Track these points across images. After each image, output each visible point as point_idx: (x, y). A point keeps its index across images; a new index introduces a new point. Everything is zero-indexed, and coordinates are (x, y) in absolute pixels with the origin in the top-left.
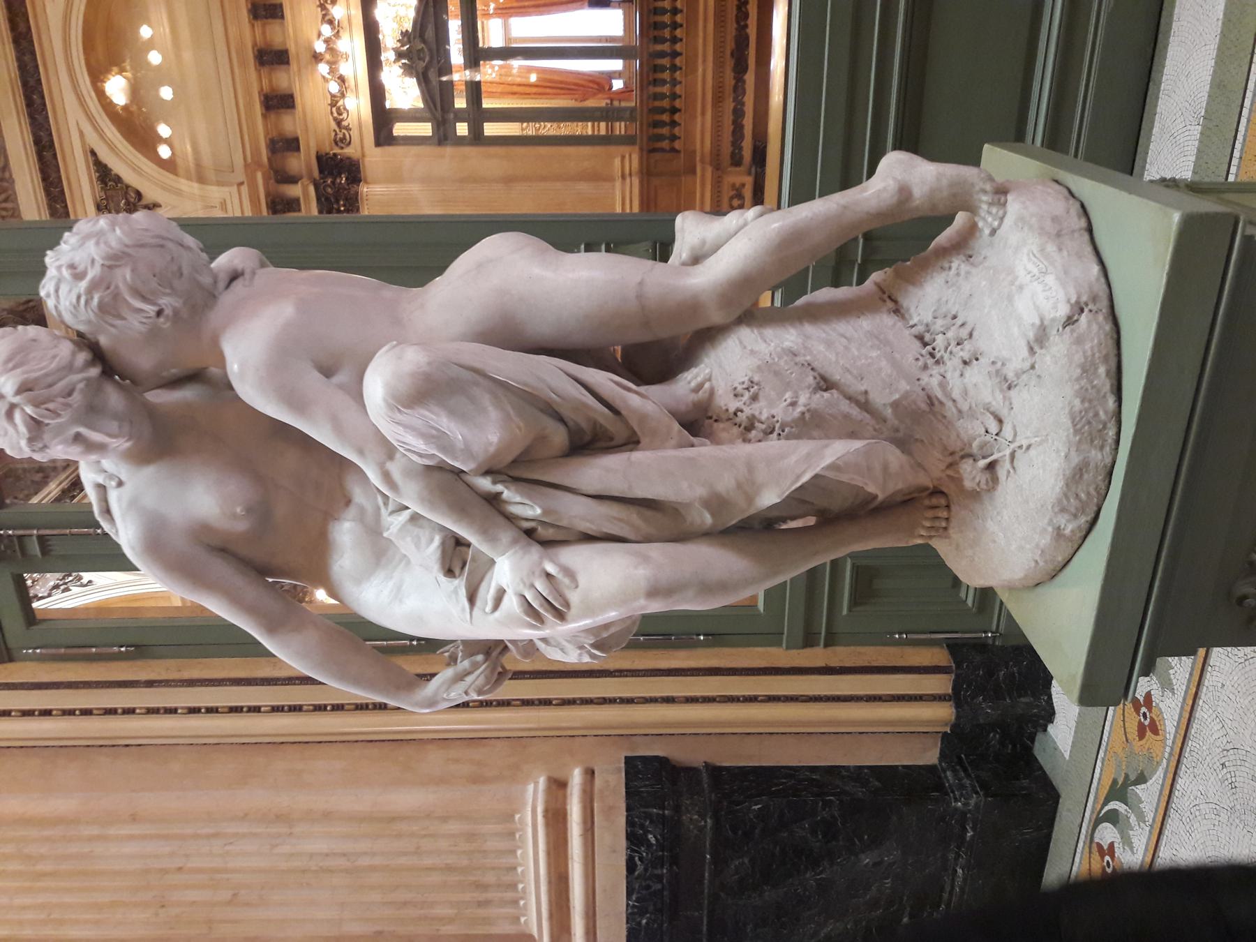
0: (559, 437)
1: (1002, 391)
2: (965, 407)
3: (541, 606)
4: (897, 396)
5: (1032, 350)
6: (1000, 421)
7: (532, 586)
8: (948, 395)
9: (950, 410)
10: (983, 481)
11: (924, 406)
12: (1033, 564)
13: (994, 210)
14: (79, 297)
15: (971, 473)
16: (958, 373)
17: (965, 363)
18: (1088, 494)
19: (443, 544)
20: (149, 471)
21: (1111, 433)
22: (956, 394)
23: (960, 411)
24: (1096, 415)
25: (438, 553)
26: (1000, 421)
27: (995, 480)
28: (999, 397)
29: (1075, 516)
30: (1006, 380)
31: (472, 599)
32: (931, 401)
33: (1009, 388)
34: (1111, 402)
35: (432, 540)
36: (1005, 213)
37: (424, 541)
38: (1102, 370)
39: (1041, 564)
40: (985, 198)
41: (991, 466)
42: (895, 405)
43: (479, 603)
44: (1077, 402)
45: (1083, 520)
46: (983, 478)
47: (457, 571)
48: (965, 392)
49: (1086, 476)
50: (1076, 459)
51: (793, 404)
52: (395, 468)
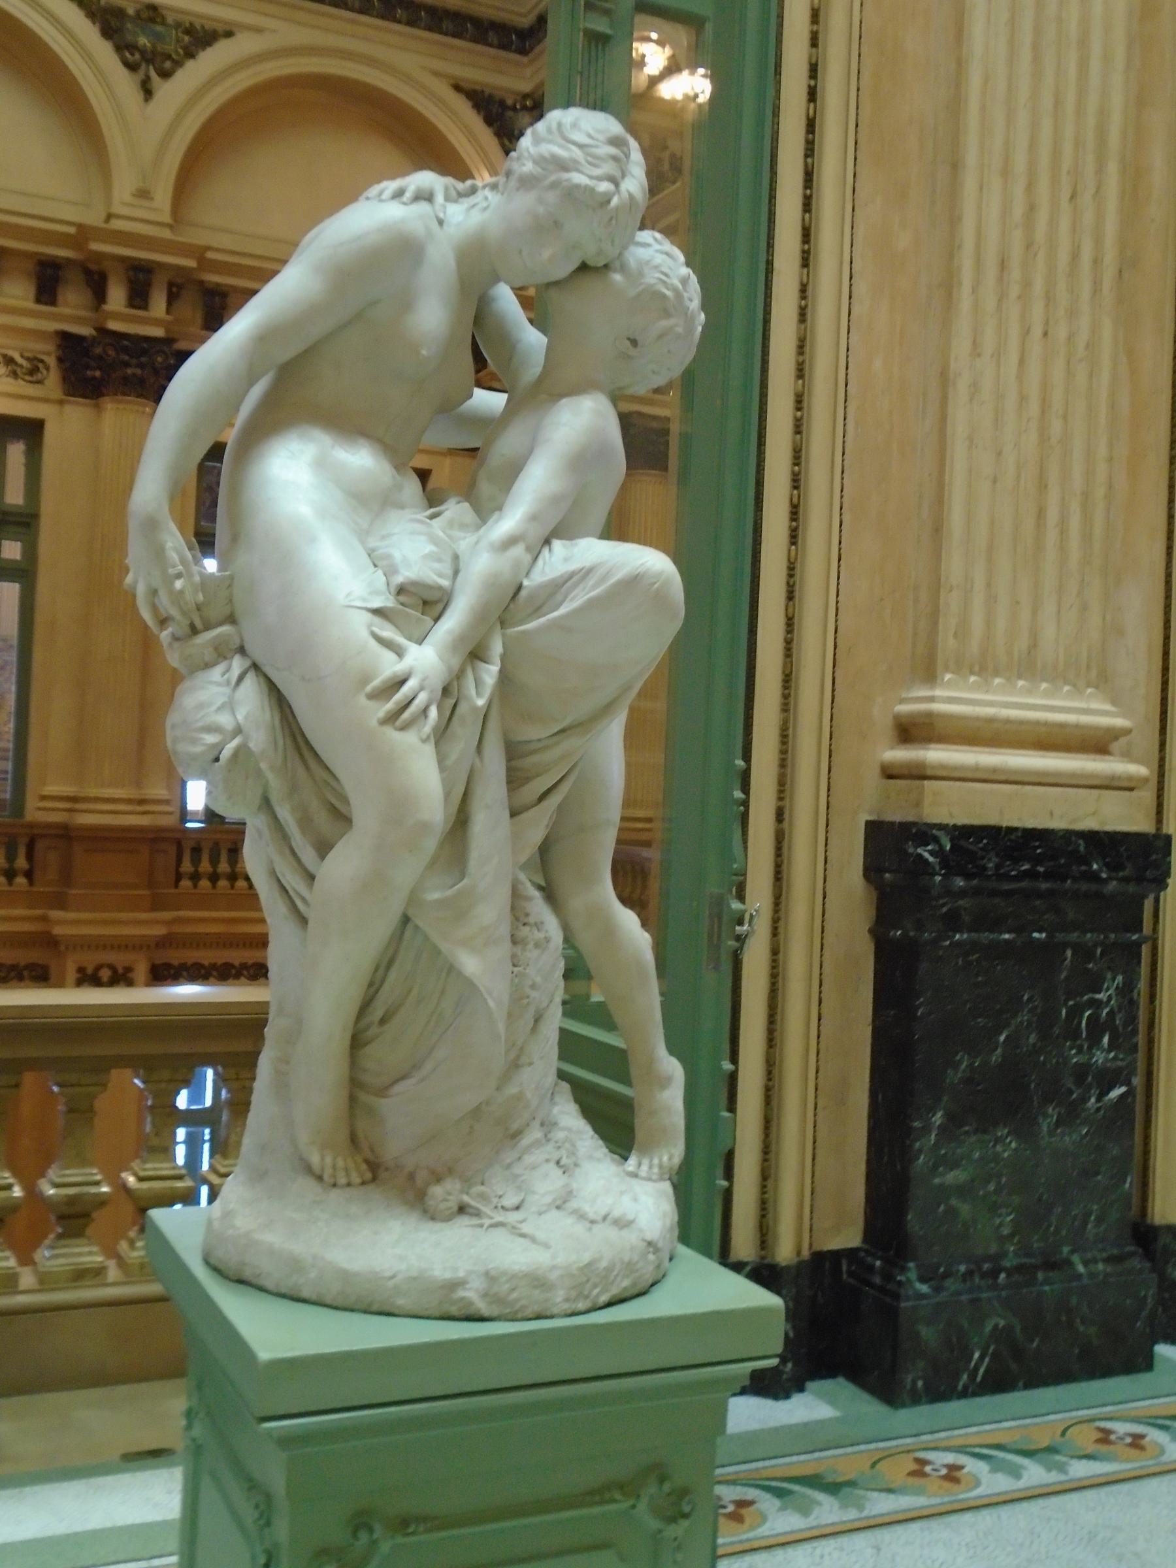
0: (533, 732)
1: (554, 1200)
2: (517, 1169)
3: (406, 697)
4: (529, 1095)
5: (605, 1218)
6: (517, 1208)
7: (422, 689)
8: (528, 1149)
9: (509, 1156)
10: (449, 1204)
11: (515, 1126)
12: (388, 1274)
13: (656, 1170)
14: (666, 275)
15: (442, 1193)
16: (547, 1156)
17: (558, 1163)
18: (517, 1300)
19: (440, 588)
20: (452, 263)
21: (581, 1306)
22: (529, 1159)
23: (509, 1166)
24: (595, 1286)
25: (430, 582)
26: (517, 1208)
27: (448, 1219)
28: (548, 1199)
29: (485, 1295)
30: (564, 1202)
31: (377, 612)
32: (516, 1135)
33: (558, 1208)
34: (604, 1299)
35: (440, 575)
36: (655, 1181)
37: (436, 565)
38: (626, 1283)
39: (391, 1283)
40: (665, 1158)
41: (462, 1209)
42: (519, 1097)
43: (377, 620)
44: (604, 1264)
45: (483, 1308)
46: (453, 1204)
47: (402, 598)
48: (534, 1167)
49: (537, 1292)
50: (553, 1276)
51: (533, 986)
52: (518, 551)
